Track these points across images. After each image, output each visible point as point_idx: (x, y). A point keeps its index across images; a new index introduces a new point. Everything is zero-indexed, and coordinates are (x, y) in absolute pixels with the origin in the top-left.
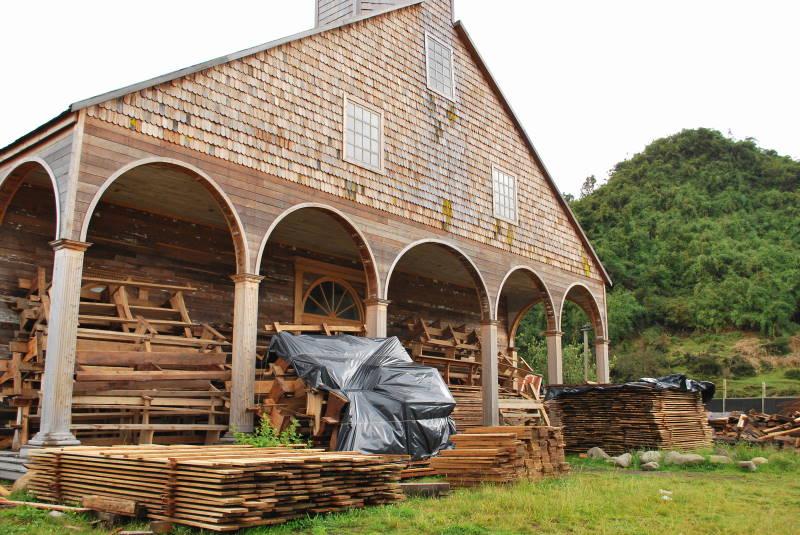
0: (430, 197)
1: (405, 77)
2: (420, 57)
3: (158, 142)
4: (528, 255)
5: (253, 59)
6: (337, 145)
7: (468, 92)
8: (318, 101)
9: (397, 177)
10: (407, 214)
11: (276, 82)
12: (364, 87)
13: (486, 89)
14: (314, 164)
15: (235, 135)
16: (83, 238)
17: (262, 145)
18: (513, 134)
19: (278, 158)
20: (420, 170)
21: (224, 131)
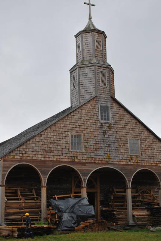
1: (91, 121)
2: (97, 112)
3: (19, 160)
4: (146, 164)
5: (42, 132)
6: (67, 148)
7: (117, 117)
8: (61, 137)
9: (89, 151)
10: (93, 161)
11: (48, 136)
12: (76, 129)
13: (126, 113)
15: (38, 153)
16: (4, 184)
17: (46, 154)
18: (138, 125)
19: (50, 156)
20: (98, 147)
21: (35, 153)
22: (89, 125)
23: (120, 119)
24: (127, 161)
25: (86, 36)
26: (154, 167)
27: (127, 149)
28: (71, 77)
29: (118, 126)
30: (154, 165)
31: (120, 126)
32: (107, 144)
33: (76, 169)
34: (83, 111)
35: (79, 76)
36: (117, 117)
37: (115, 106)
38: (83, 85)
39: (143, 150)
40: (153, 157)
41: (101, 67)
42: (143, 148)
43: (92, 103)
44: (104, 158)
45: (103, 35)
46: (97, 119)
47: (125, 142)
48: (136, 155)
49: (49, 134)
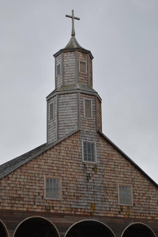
0: (84, 204)
1: (72, 161)
4: (139, 217)
6: (41, 194)
7: (104, 157)
8: (34, 181)
9: (68, 200)
10: (73, 213)
12: (53, 171)
13: (115, 153)
14: (32, 203)
17: (13, 202)
19: (19, 205)
20: (79, 195)
22: (69, 167)
23: (108, 160)
24: (117, 213)
25: (68, 55)
26: (150, 222)
27: (116, 198)
28: (48, 106)
29: (105, 168)
30: (150, 218)
31: (108, 169)
32: (91, 191)
33: (50, 221)
34: (62, 148)
35: (58, 105)
36: (104, 157)
37: (102, 143)
38: (63, 117)
39: (136, 200)
40: (149, 208)
41: (85, 94)
42: (136, 197)
43: (73, 139)
44: (88, 209)
45: (88, 55)
46: (80, 160)
47: (113, 189)
48: (128, 205)
49: (19, 177)
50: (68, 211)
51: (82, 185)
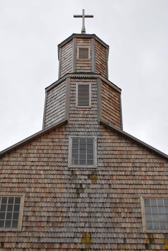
0: (67, 235)
1: (46, 168)
7: (113, 157)
9: (35, 229)
13: (134, 148)
20: (60, 219)
27: (139, 220)
32: (84, 212)
37: (109, 137)
38: (51, 115)
41: (79, 78)
43: (54, 137)
44: (75, 243)
45: (92, 39)
50: (33, 248)
51: (65, 202)
